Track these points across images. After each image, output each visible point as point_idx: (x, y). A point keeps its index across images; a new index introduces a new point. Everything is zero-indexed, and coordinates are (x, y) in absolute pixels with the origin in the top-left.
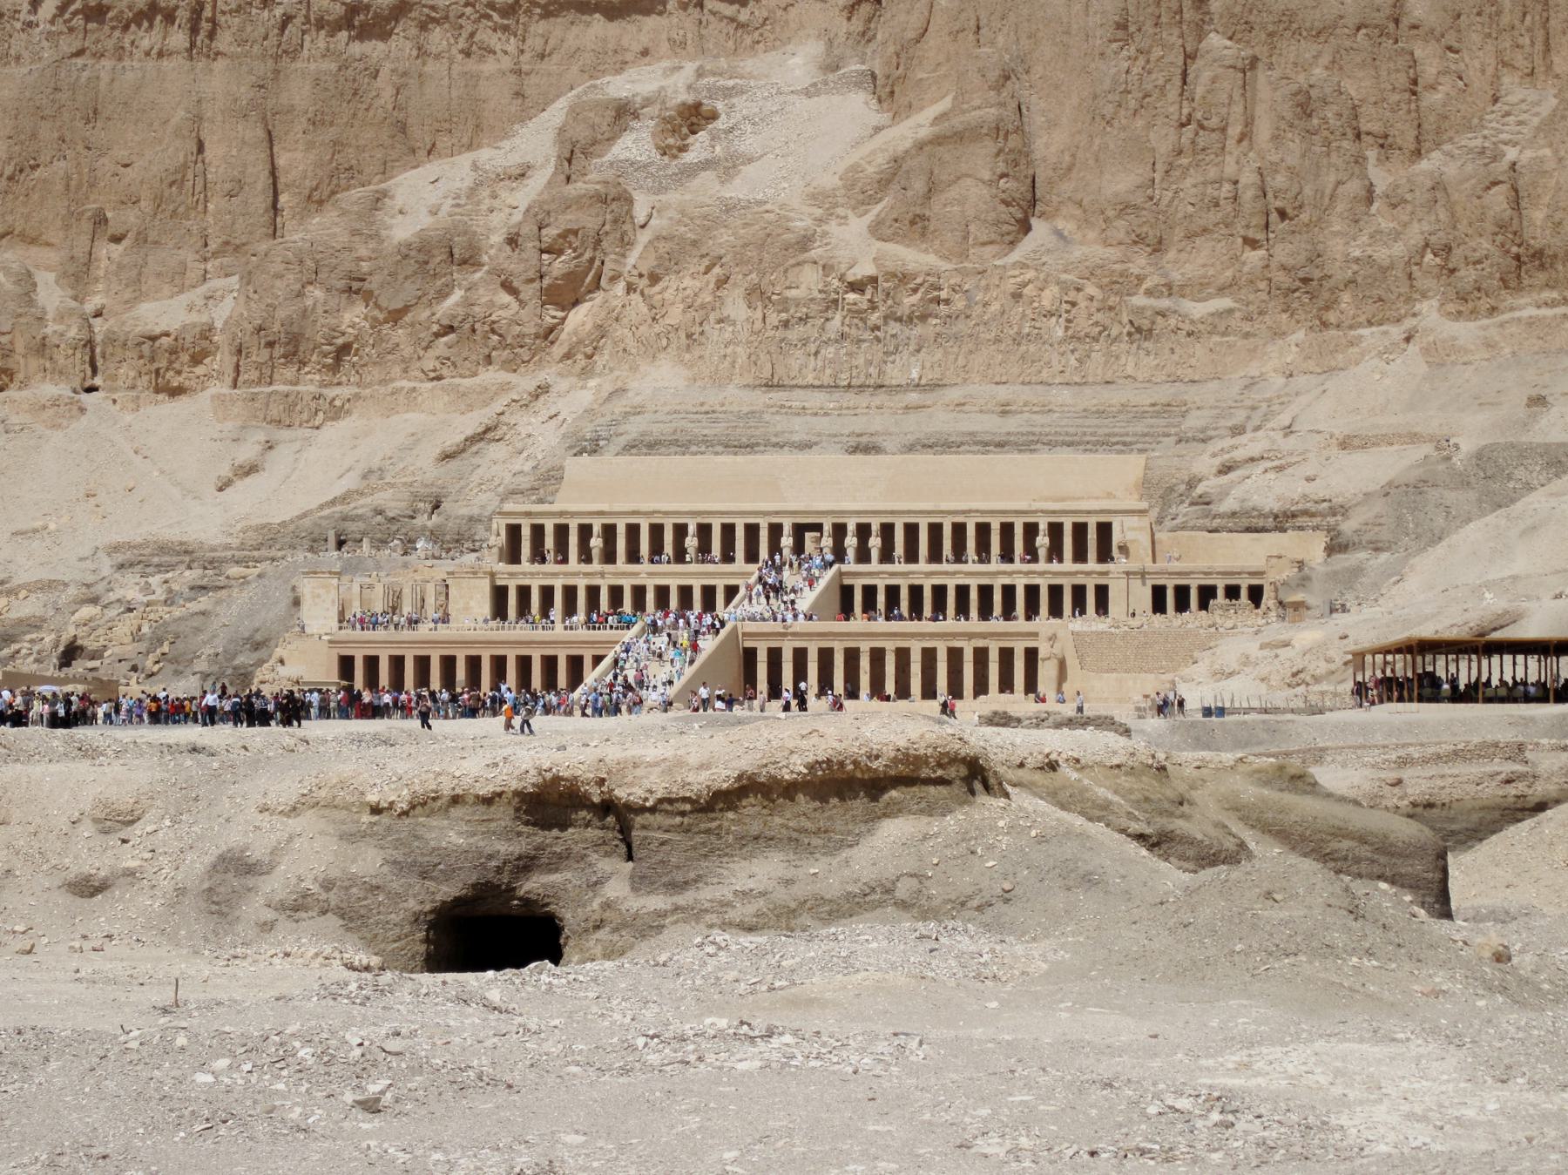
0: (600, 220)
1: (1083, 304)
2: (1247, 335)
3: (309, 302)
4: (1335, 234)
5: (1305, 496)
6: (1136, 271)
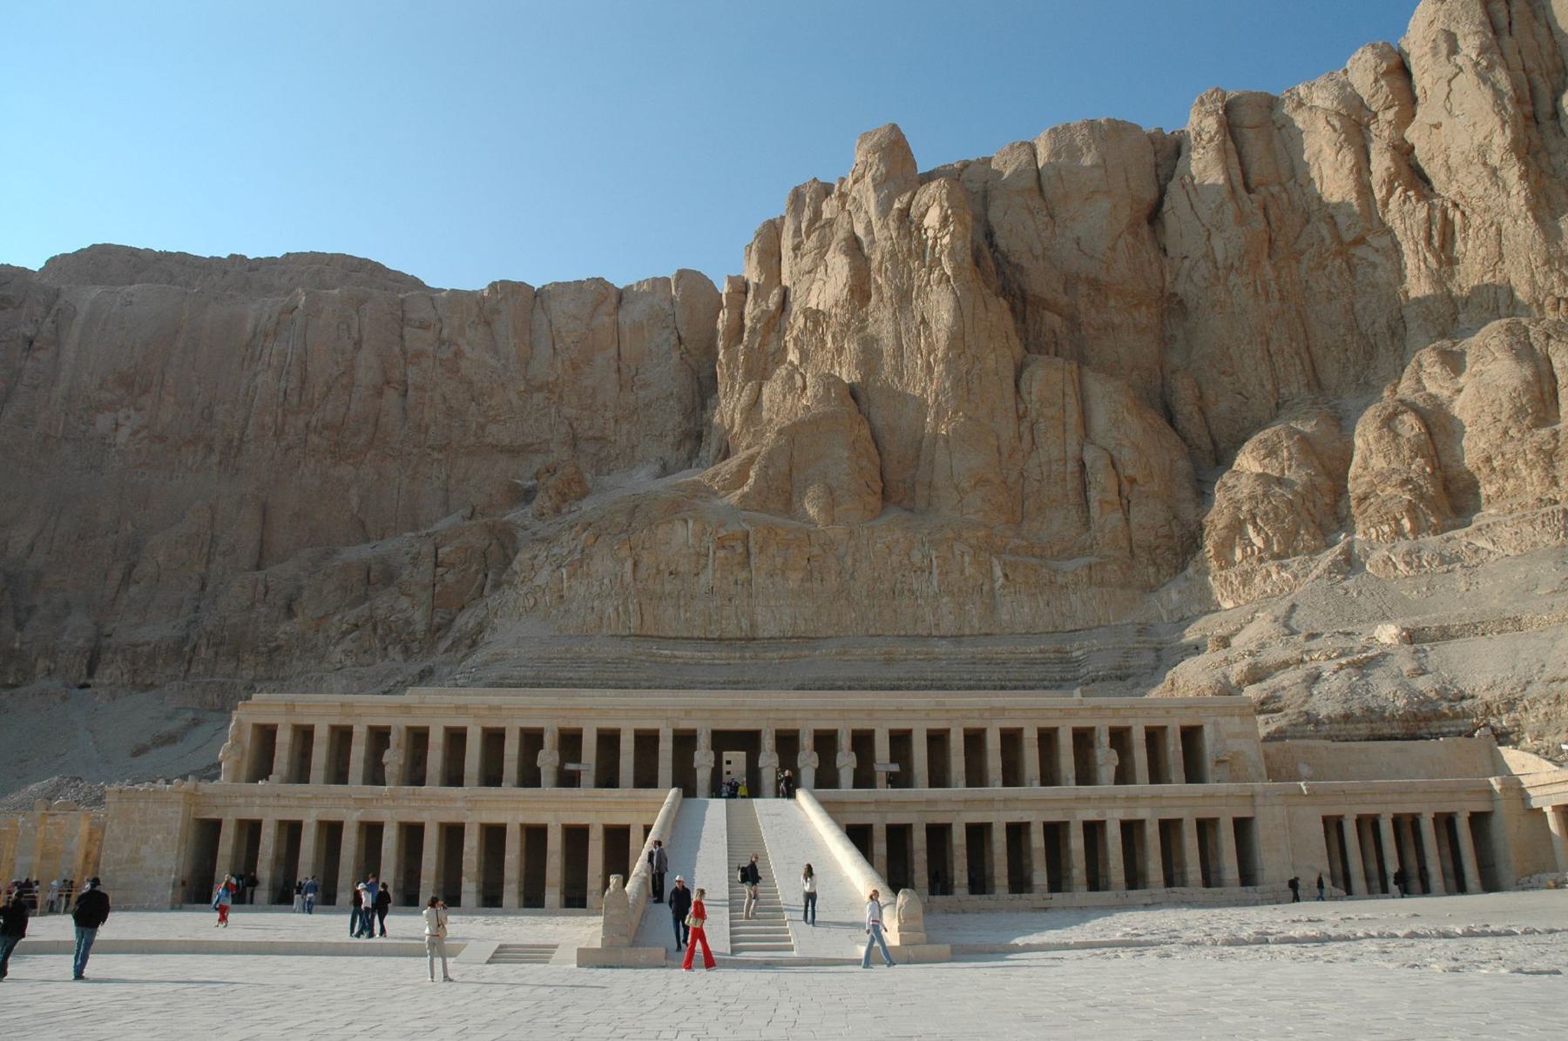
0: (487, 542)
3: (254, 615)
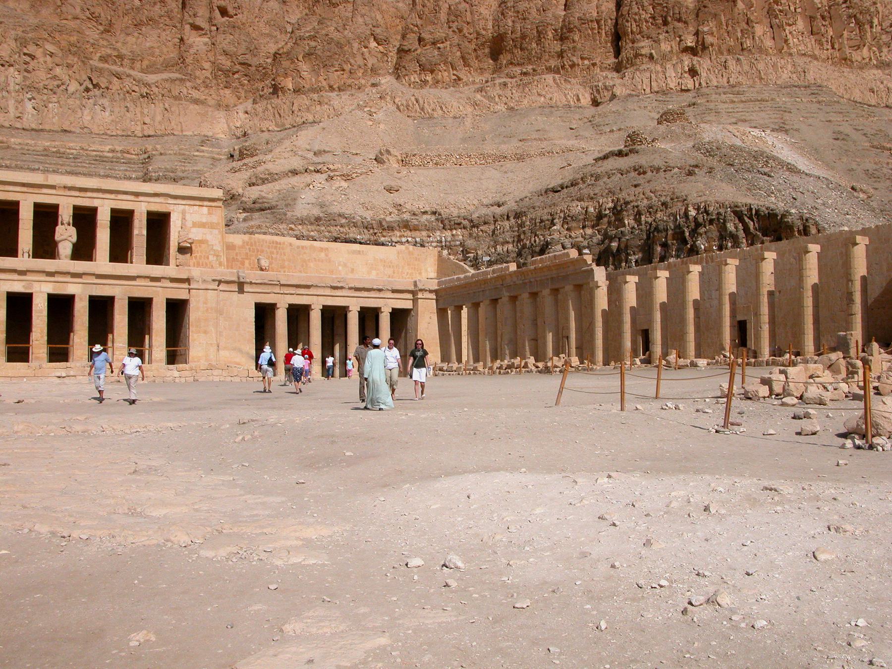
1: (41, 60)
2: (196, 102)
4: (268, 35)
5: (398, 207)
6: (92, 41)
